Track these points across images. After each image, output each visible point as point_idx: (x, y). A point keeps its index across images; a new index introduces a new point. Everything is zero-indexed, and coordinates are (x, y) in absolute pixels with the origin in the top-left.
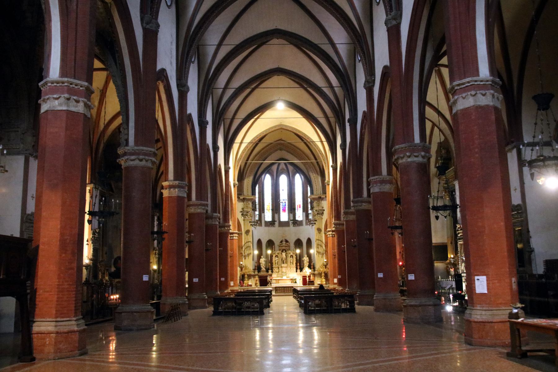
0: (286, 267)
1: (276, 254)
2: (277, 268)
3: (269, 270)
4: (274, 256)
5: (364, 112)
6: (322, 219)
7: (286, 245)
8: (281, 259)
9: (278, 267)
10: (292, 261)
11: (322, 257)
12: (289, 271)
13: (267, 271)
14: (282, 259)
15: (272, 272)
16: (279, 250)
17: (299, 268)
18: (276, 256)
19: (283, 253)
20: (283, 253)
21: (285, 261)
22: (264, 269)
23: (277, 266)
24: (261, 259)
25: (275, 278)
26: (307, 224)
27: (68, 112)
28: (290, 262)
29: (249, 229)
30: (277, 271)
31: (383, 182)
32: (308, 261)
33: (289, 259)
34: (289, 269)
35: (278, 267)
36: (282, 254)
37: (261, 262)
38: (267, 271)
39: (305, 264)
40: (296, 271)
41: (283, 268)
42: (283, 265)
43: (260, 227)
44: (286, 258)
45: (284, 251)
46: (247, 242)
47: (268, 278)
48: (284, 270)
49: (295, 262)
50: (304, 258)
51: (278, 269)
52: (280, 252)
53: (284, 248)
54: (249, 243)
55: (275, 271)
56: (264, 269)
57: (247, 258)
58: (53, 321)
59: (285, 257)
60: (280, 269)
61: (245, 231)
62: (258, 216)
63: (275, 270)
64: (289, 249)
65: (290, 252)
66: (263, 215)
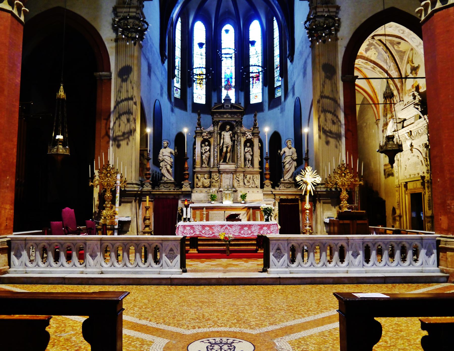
0: (234, 172)
2: (206, 176)
3: (185, 179)
6: (337, 39)
8: (217, 149)
9: (210, 173)
10: (249, 157)
11: (336, 147)
12: (242, 184)
13: (178, 183)
14: (221, 150)
15: (193, 186)
17: (268, 176)
18: (203, 142)
19: (223, 133)
20: (223, 133)
21: (228, 155)
23: (207, 169)
24: (162, 150)
25: (201, 201)
26: (270, 108)
28: (245, 159)
29: (129, 63)
30: (207, 182)
32: (295, 156)
33: (241, 150)
34: (241, 177)
35: (210, 173)
37: (161, 157)
38: (178, 183)
39: (287, 166)
40: (262, 186)
41: (224, 176)
42: (223, 167)
43: (183, 112)
44: (233, 146)
45: (228, 127)
46: (122, 101)
47: (180, 202)
48: (226, 180)
49: (257, 160)
50: (285, 149)
51: (210, 177)
52: (217, 129)
53: (227, 118)
54: (131, 102)
55: (200, 184)
56: (169, 177)
57: (123, 143)
60: (215, 176)
61: (120, 67)
62: (179, 91)
63: (203, 180)
65: (244, 129)
66: (189, 90)
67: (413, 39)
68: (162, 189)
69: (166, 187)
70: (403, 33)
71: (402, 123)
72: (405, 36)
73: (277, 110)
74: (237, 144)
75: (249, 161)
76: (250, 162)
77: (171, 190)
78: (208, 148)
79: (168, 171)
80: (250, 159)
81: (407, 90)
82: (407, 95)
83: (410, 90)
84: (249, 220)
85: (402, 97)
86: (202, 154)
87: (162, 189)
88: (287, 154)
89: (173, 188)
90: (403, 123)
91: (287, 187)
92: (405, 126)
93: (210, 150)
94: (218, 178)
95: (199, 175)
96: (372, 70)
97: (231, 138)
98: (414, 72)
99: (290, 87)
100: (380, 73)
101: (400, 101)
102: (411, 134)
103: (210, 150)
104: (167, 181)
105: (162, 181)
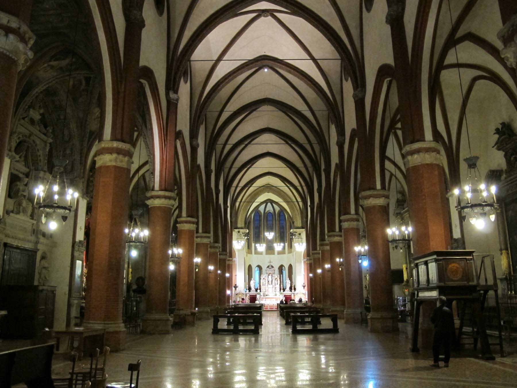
1: (264, 277)
4: (262, 278)
5: (336, 164)
10: (276, 283)
13: (256, 290)
15: (260, 291)
22: (253, 289)
27: (116, 167)
31: (352, 220)
38: (256, 290)
39: (287, 286)
44: (272, 280)
45: (270, 275)
52: (267, 275)
53: (270, 272)
58: (102, 323)
59: (271, 280)
64: (274, 273)
73: (291, 254)
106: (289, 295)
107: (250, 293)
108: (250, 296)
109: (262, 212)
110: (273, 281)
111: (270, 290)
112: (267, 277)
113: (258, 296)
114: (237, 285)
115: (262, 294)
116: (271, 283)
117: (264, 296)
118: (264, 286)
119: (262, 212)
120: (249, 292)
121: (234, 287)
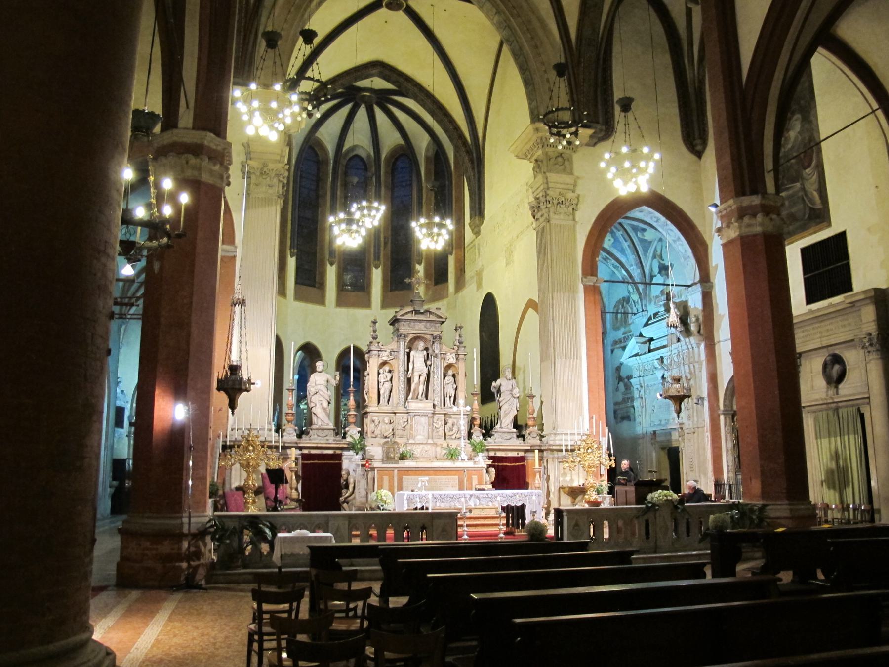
1: (385, 356)
7: (432, 318)
16: (400, 336)
19: (412, 353)
36: (409, 355)
38: (340, 428)
42: (413, 405)
45: (421, 345)
53: (419, 329)
65: (445, 349)
67: (669, 231)
68: (314, 439)
69: (321, 435)
70: (657, 221)
71: (648, 343)
72: (659, 226)
74: (434, 372)
75: (450, 397)
76: (452, 399)
77: (331, 441)
78: (389, 375)
79: (324, 409)
80: (453, 395)
81: (654, 297)
82: (653, 303)
83: (657, 297)
84: (461, 488)
85: (646, 306)
86: (378, 382)
87: (314, 439)
88: (502, 389)
89: (333, 438)
90: (650, 344)
91: (506, 438)
92: (652, 348)
93: (391, 380)
94: (406, 423)
95: (376, 419)
96: (604, 261)
97: (425, 361)
98: (663, 272)
99: (469, 272)
100: (614, 268)
101: (643, 311)
102: (662, 362)
103: (391, 380)
104: (323, 427)
105: (313, 427)
106: (514, 454)
107: (305, 442)
108: (305, 457)
109: (330, 147)
110: (436, 379)
111: (421, 428)
112: (402, 357)
113: (350, 463)
114: (244, 374)
115: (375, 449)
116: (422, 388)
117: (387, 458)
118: (384, 406)
119: (330, 147)
120: (299, 436)
121: (222, 386)
